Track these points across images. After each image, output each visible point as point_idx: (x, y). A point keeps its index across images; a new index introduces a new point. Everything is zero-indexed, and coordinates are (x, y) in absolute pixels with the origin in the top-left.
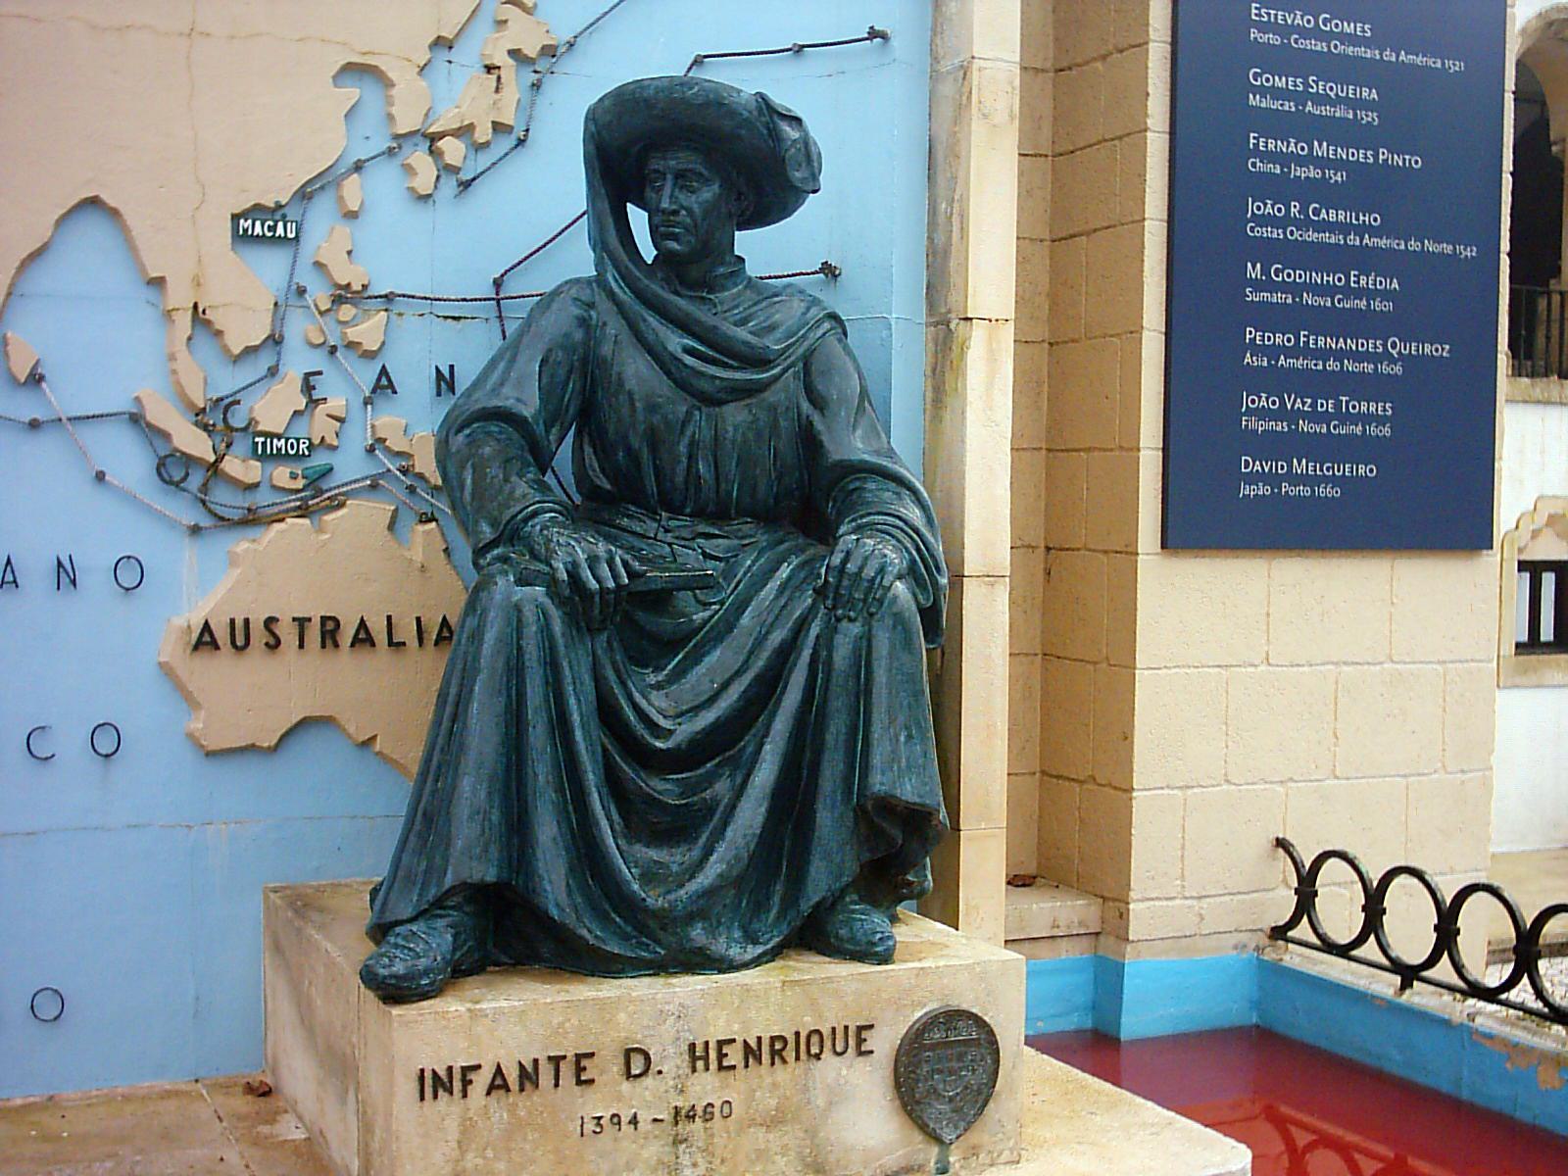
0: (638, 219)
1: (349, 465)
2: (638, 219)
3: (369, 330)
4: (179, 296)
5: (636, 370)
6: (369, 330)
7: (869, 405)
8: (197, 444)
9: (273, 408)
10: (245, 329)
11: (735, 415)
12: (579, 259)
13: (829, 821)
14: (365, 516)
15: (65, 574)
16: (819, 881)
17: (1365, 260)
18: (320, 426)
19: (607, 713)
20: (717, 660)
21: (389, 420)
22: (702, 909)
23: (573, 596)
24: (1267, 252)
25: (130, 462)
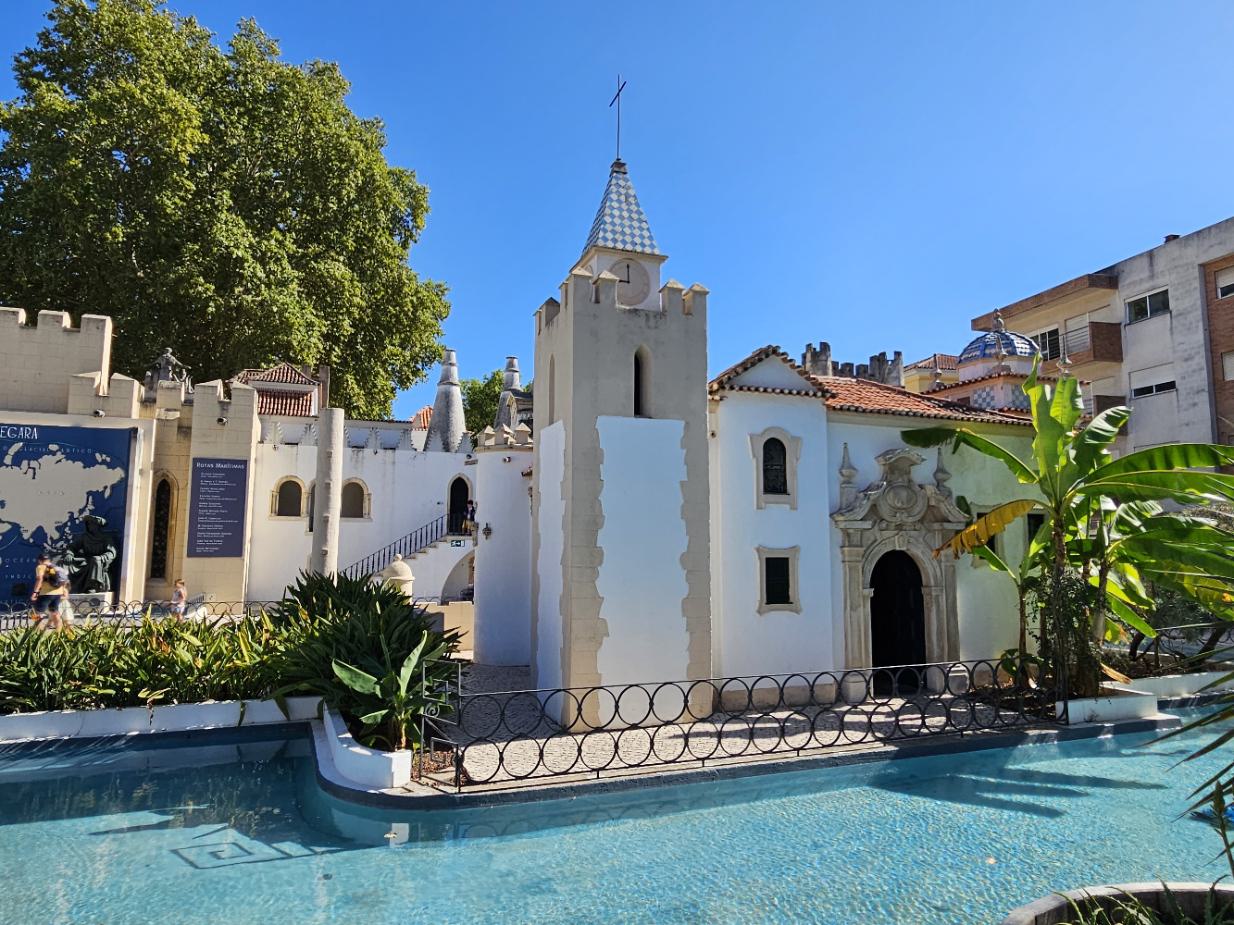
17: (217, 523)
24: (201, 523)
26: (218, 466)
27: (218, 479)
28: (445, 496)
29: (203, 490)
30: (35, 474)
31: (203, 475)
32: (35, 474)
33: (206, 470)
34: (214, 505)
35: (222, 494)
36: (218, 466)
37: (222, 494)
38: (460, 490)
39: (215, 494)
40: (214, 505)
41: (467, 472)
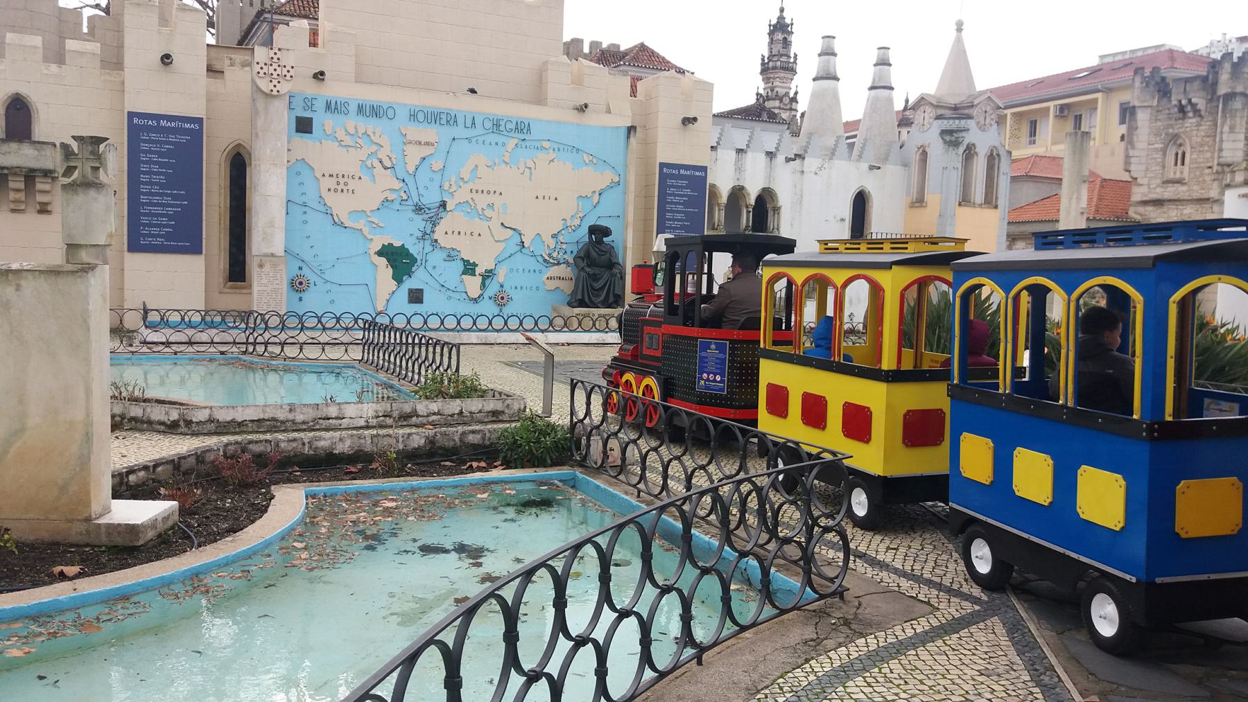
0: (593, 236)
1: (562, 261)
2: (593, 236)
3: (564, 246)
4: (546, 243)
5: (594, 253)
6: (564, 246)
7: (616, 256)
8: (548, 258)
9: (555, 255)
10: (552, 246)
11: (603, 257)
12: (586, 239)
13: (611, 295)
14: (563, 266)
15: (535, 271)
16: (610, 301)
18: (559, 257)
19: (591, 285)
20: (601, 281)
21: (566, 256)
22: (599, 303)
23: (588, 274)
25: (540, 259)
26: (682, 172)
27: (681, 187)
28: (847, 212)
29: (669, 199)
30: (531, 174)
31: (669, 182)
32: (531, 174)
33: (672, 176)
34: (679, 216)
35: (684, 204)
36: (682, 172)
37: (684, 204)
38: (861, 202)
39: (679, 204)
40: (679, 216)
41: (871, 184)
